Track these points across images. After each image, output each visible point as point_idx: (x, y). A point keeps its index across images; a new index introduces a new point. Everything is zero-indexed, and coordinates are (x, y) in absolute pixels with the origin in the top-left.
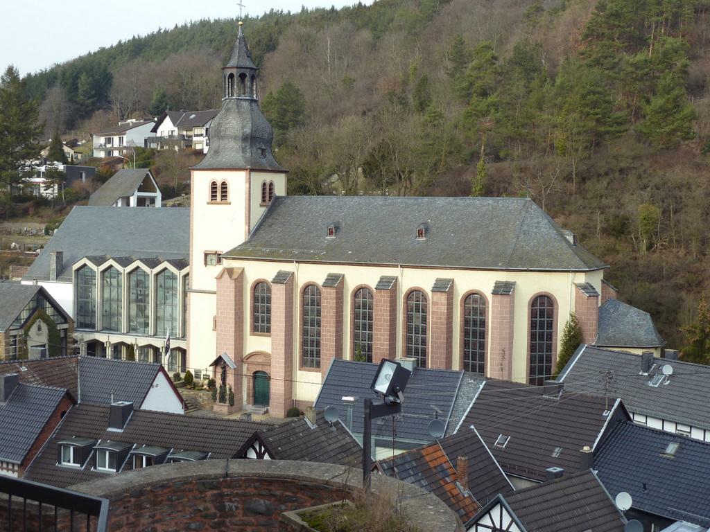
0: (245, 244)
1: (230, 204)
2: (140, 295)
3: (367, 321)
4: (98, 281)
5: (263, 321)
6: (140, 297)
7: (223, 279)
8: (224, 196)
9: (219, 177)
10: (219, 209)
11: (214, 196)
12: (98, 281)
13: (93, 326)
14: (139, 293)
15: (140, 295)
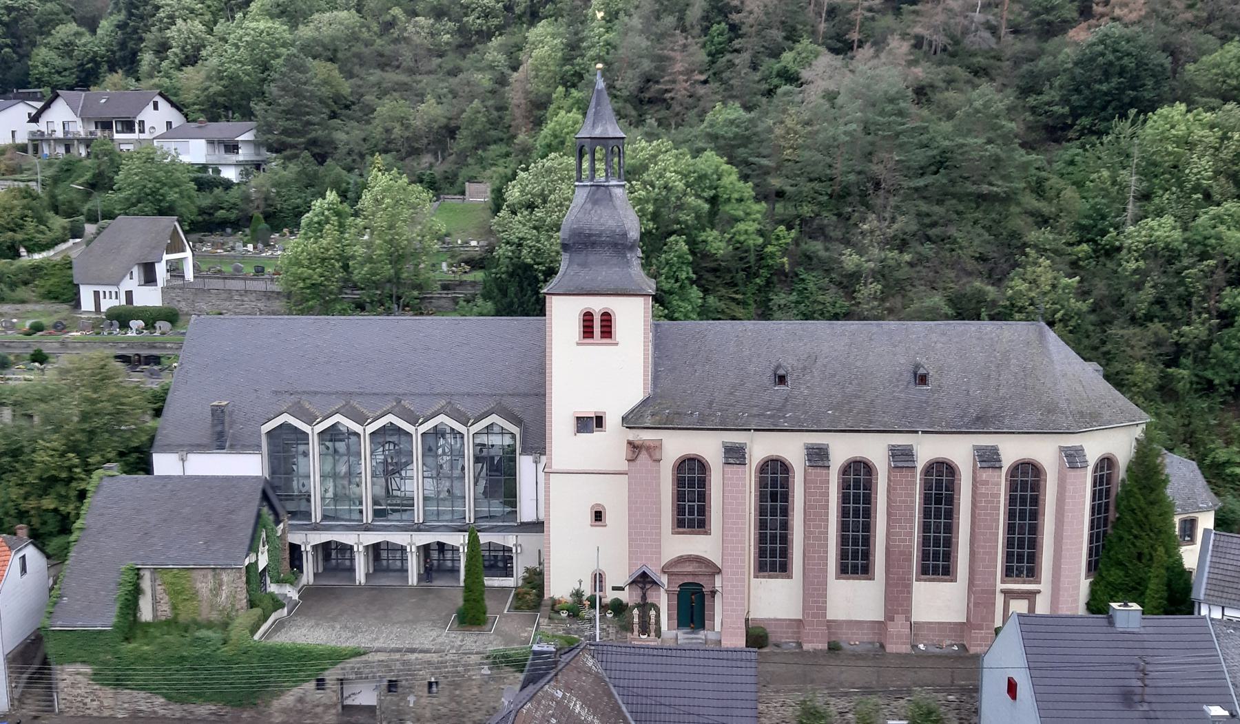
0: (644, 403)
1: (617, 344)
2: (391, 464)
3: (861, 506)
4: (314, 447)
5: (691, 513)
6: (390, 468)
7: (638, 462)
8: (607, 332)
9: (597, 305)
10: (597, 351)
11: (588, 331)
12: (314, 447)
13: (307, 515)
14: (389, 461)
15: (391, 464)
